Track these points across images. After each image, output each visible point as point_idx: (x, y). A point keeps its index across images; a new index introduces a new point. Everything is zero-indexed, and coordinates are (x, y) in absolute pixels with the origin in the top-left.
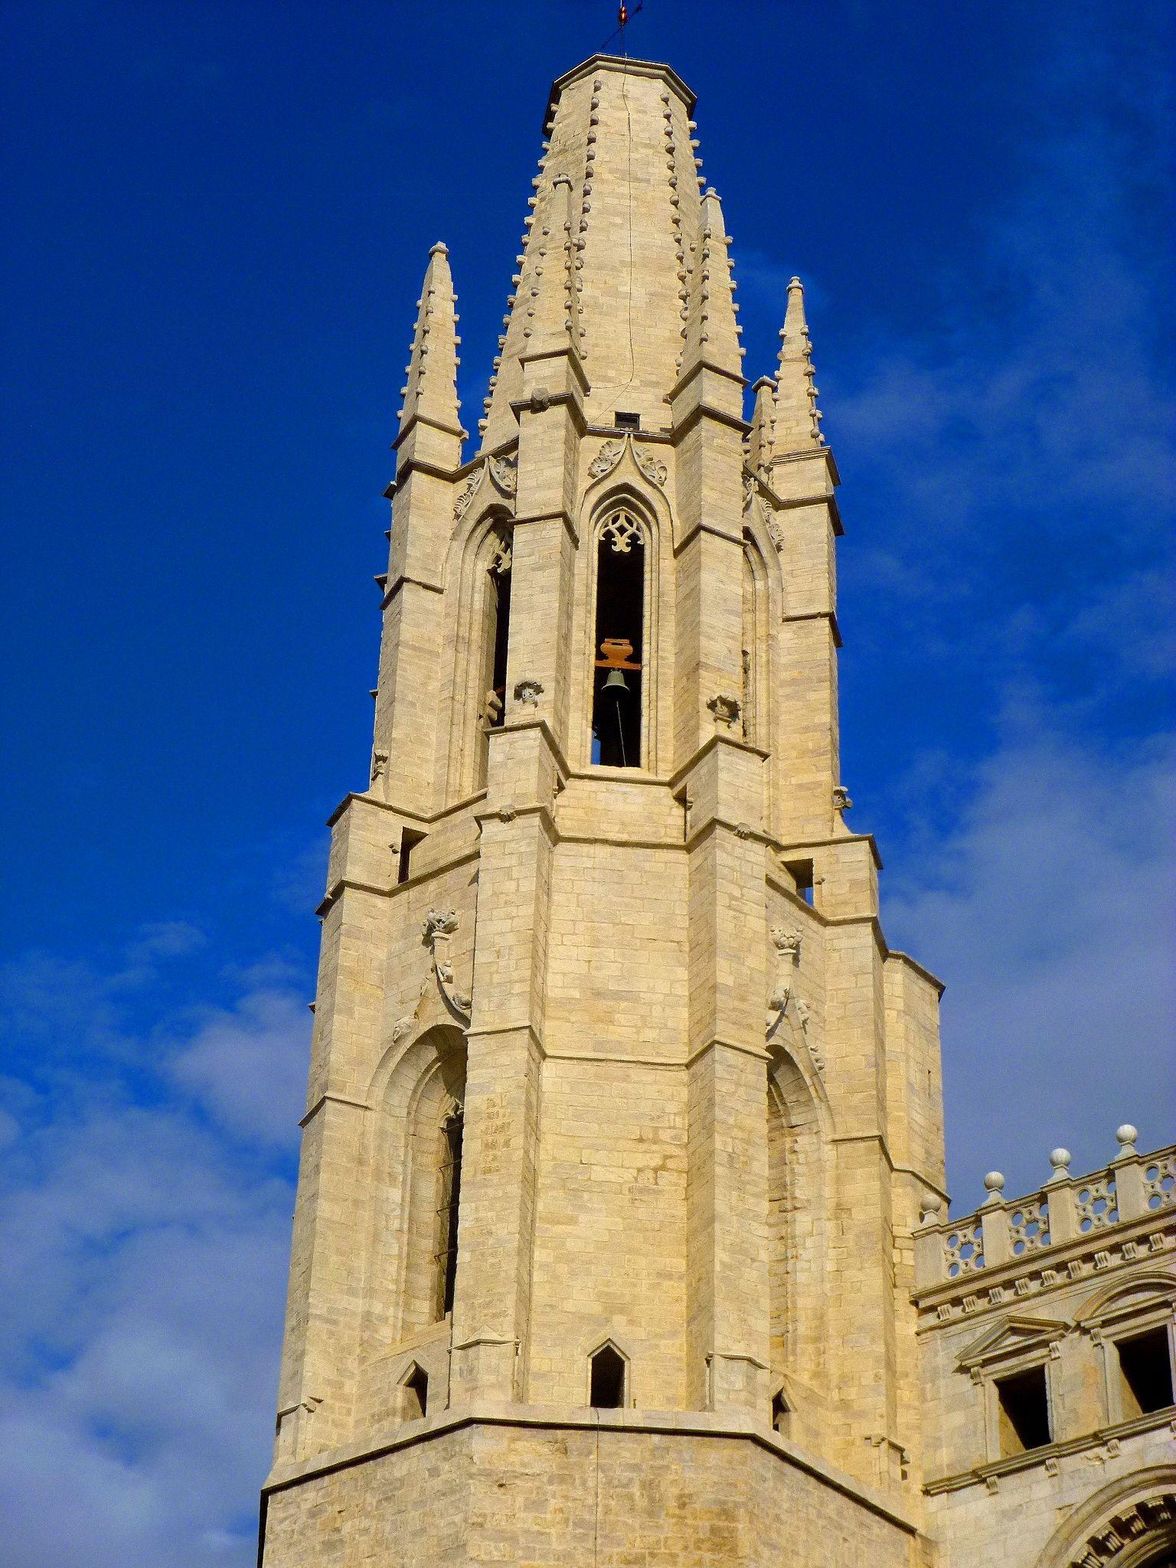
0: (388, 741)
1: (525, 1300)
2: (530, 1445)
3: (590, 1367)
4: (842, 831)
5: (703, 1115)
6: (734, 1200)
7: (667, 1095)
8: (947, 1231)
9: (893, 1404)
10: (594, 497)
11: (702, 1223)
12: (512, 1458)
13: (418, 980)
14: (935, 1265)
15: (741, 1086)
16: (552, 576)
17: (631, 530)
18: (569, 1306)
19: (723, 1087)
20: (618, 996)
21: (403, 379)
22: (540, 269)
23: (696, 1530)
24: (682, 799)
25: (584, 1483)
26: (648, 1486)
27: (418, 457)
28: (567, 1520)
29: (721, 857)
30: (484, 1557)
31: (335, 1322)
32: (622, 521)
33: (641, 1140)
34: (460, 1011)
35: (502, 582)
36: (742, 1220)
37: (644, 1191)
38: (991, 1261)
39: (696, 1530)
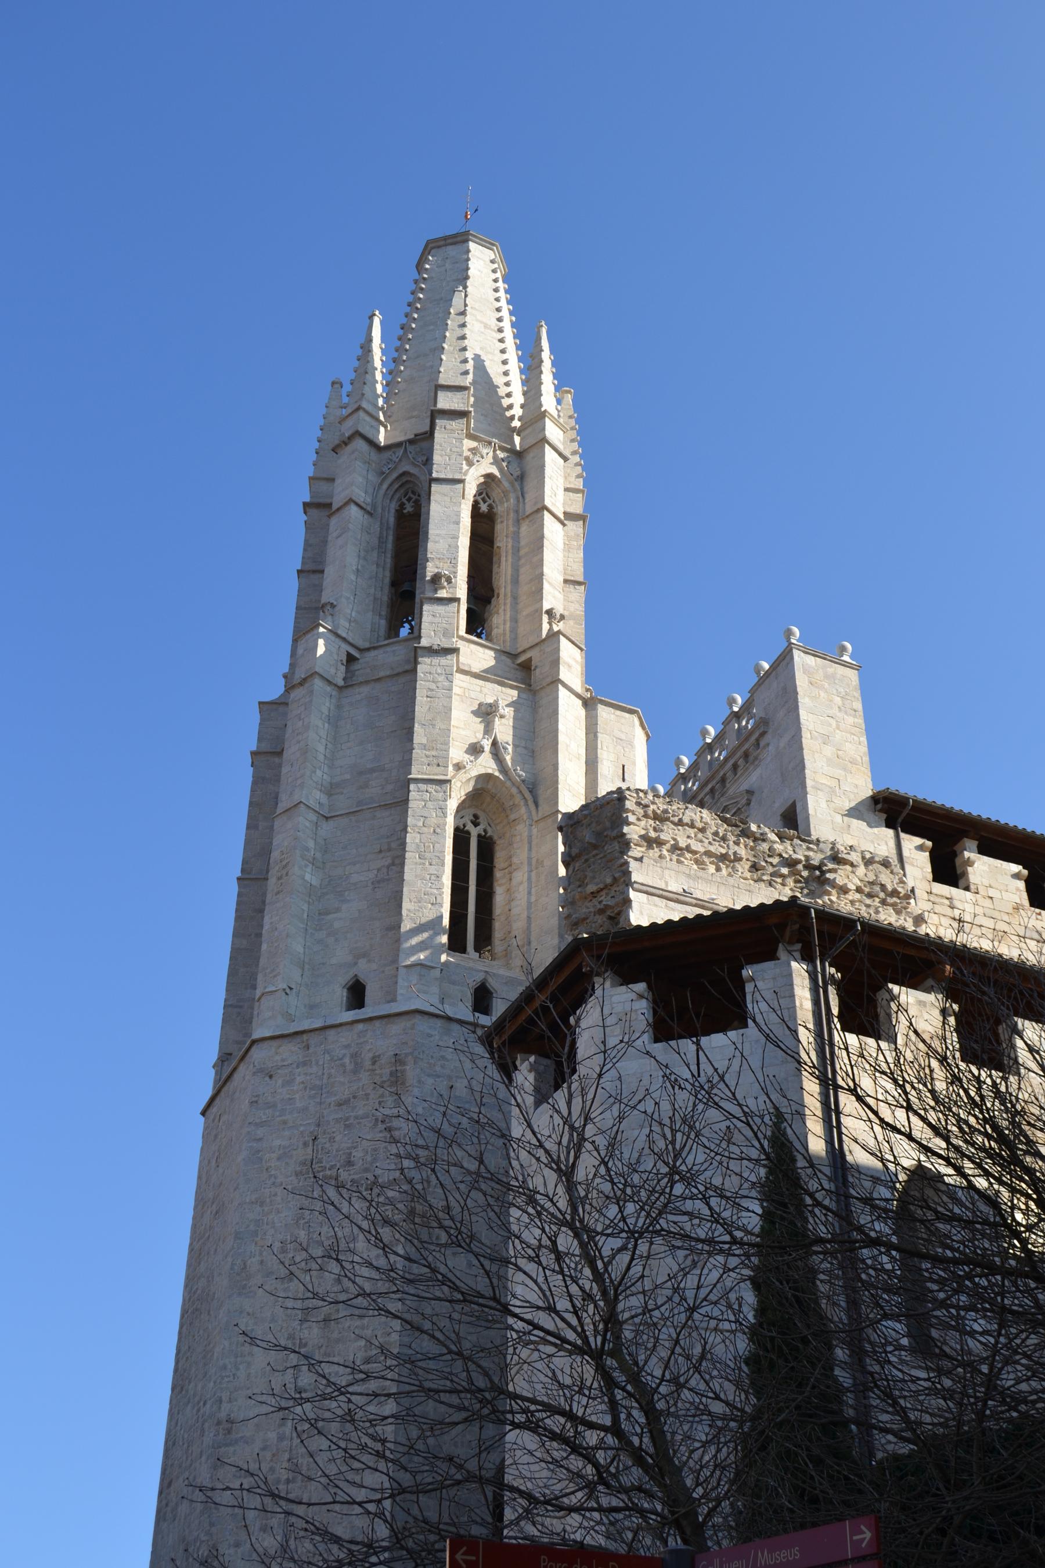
3: (345, 994)
6: (419, 872)
10: (385, 486)
12: (278, 1058)
17: (414, 498)
18: (334, 961)
20: (372, 770)
23: (381, 1076)
25: (317, 1063)
26: (354, 1056)
28: (305, 1088)
30: (258, 1121)
31: (241, 1007)
32: (410, 494)
33: (380, 851)
37: (383, 880)
39: (381, 1076)
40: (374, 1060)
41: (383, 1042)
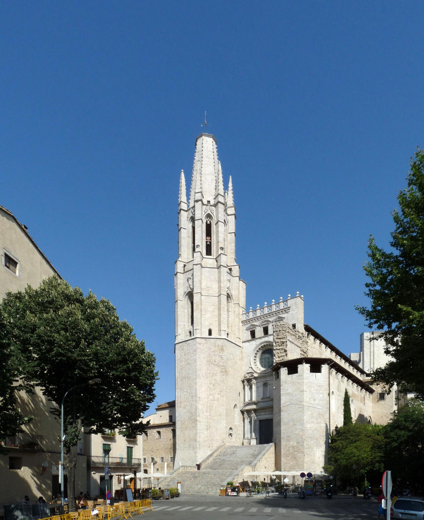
0: (181, 252)
1: (201, 324)
2: (202, 340)
4: (235, 264)
5: (220, 301)
7: (216, 299)
8: (245, 314)
9: (239, 333)
11: (220, 315)
13: (187, 285)
14: (244, 318)
15: (224, 298)
16: (200, 228)
19: (222, 299)
20: (210, 287)
21: (179, 194)
22: (196, 176)
24: (217, 261)
26: (215, 344)
27: (182, 208)
29: (222, 270)
34: (193, 290)
35: (194, 228)
36: (224, 314)
38: (250, 318)
40: (218, 345)
41: (220, 342)
